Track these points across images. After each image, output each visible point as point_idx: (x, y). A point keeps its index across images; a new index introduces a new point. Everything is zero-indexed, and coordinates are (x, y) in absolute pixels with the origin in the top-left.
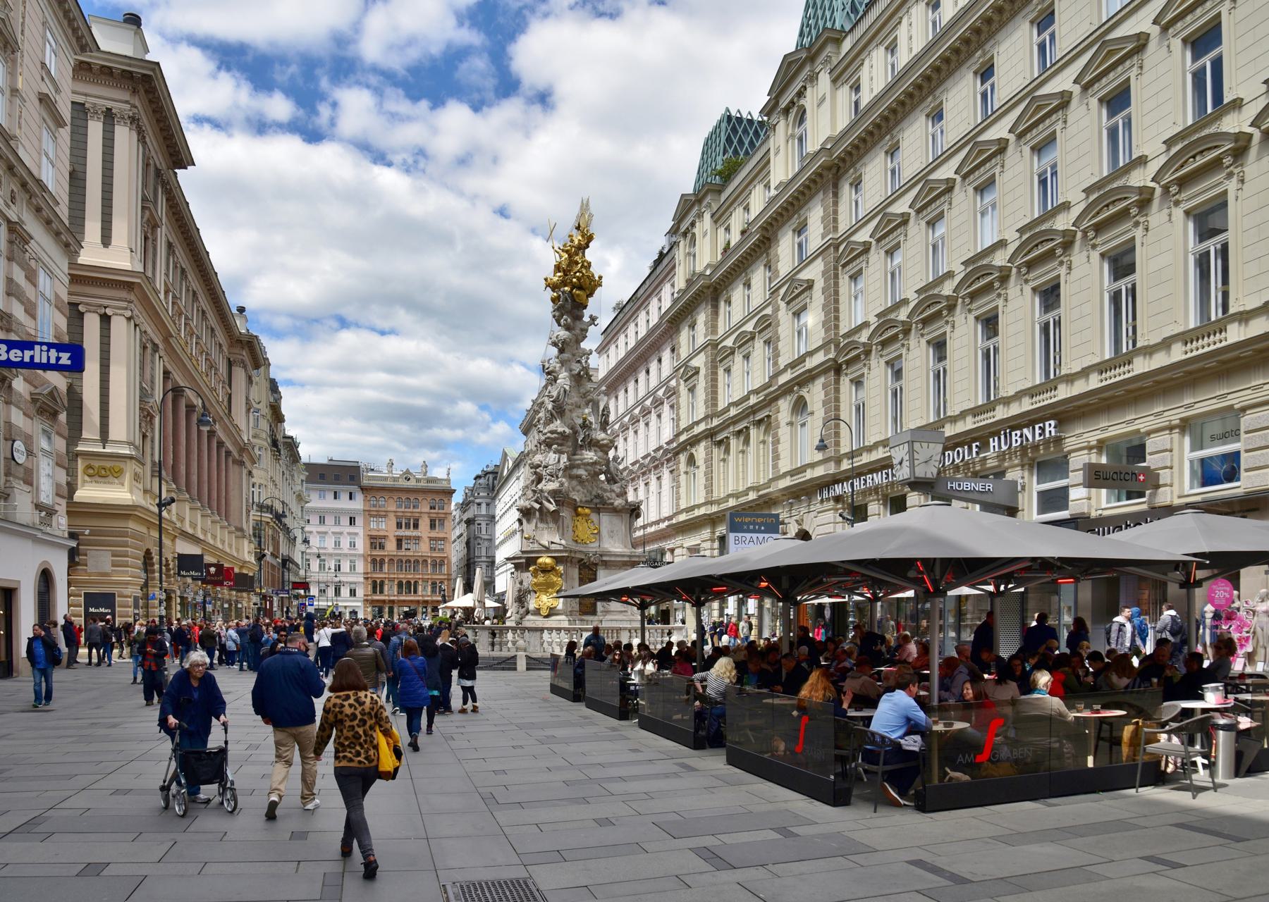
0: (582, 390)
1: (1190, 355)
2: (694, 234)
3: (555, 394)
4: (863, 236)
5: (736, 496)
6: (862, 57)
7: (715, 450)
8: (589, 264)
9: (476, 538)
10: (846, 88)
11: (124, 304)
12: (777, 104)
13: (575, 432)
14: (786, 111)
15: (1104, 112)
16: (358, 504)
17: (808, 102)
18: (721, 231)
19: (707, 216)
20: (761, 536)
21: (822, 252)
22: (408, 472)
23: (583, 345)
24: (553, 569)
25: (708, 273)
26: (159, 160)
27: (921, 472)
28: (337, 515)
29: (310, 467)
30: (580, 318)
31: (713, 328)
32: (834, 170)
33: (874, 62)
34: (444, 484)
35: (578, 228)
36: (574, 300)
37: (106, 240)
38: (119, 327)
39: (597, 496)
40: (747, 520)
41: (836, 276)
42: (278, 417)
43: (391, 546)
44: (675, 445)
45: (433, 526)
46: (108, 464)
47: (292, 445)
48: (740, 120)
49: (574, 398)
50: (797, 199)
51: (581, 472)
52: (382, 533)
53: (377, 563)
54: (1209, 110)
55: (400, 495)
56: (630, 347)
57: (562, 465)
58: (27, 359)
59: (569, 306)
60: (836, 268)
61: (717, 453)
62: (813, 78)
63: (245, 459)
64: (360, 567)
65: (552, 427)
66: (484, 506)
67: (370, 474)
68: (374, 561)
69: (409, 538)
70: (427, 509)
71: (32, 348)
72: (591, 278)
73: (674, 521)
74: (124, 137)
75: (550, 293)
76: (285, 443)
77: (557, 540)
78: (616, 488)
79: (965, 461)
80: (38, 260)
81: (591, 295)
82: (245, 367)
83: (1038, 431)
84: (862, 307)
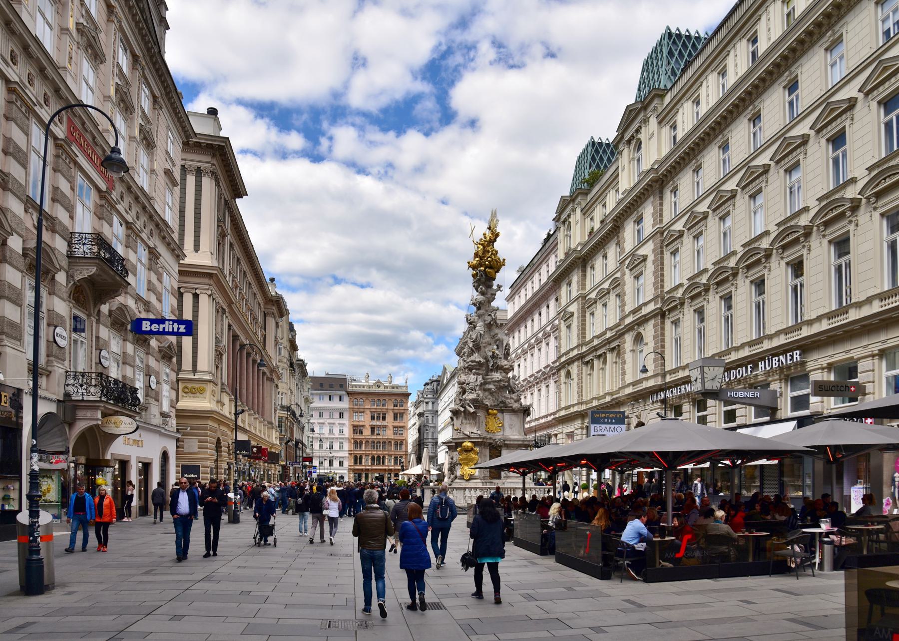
0: (492, 334)
1: (884, 308)
2: (570, 223)
3: (474, 337)
4: (679, 226)
5: (598, 399)
6: (677, 107)
7: (584, 368)
8: (497, 252)
9: (425, 426)
10: (668, 127)
11: (207, 287)
12: (622, 137)
13: (488, 361)
14: (629, 142)
15: (830, 147)
16: (345, 404)
17: (643, 136)
18: (588, 220)
19: (578, 211)
20: (612, 426)
21: (652, 236)
22: (379, 382)
23: (492, 304)
24: (472, 449)
25: (579, 249)
26: (227, 195)
27: (709, 386)
28: (331, 411)
29: (314, 379)
30: (491, 286)
31: (583, 285)
32: (660, 182)
33: (685, 111)
34: (403, 390)
35: (489, 228)
36: (486, 275)
37: (197, 248)
38: (204, 300)
39: (502, 402)
40: (603, 416)
41: (662, 253)
42: (294, 347)
43: (367, 432)
44: (558, 364)
45: (395, 418)
46: (196, 386)
47: (302, 365)
48: (600, 144)
49: (487, 339)
50: (626, 211)
51: (491, 386)
52: (361, 423)
53: (357, 444)
54: (895, 148)
55: (373, 397)
56: (528, 297)
57: (478, 383)
58: (161, 330)
59: (483, 280)
60: (661, 247)
61: (586, 370)
62: (646, 121)
63: (274, 377)
64: (347, 446)
65: (472, 358)
66: (430, 404)
67: (354, 383)
68: (355, 443)
69: (379, 426)
70: (392, 407)
71: (164, 323)
72: (498, 261)
73: (557, 416)
74: (208, 184)
75: (471, 271)
76: (298, 364)
77: (475, 431)
78: (514, 396)
79: (745, 378)
80: (163, 267)
81: (498, 271)
82: (274, 317)
83: (789, 358)
84: (679, 272)
